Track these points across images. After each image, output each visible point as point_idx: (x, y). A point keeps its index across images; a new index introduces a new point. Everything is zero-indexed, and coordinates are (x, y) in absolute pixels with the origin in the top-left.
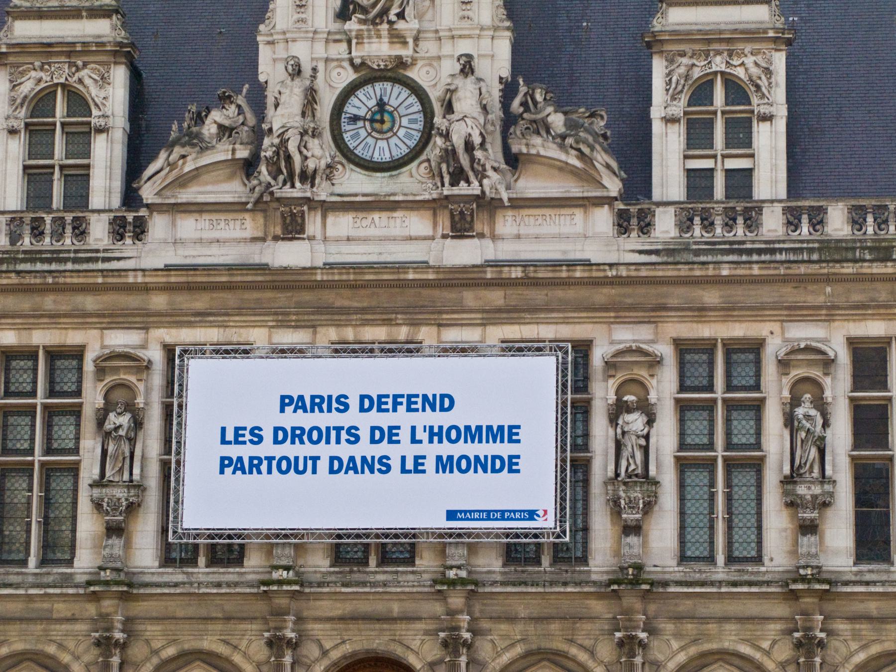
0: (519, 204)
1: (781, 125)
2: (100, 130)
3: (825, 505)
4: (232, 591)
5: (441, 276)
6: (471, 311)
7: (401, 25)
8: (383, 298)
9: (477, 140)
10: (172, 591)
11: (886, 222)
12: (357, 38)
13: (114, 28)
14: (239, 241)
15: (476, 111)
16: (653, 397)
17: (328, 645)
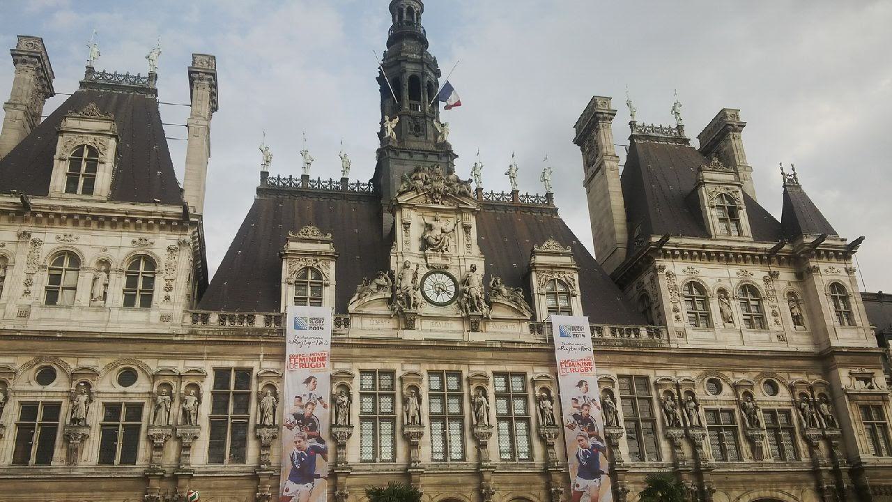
0: (495, 319)
1: (579, 298)
2: (327, 285)
3: (618, 436)
4: (393, 472)
5: (469, 345)
6: (481, 359)
7: (446, 253)
8: (447, 354)
9: (480, 296)
10: (367, 473)
11: (623, 334)
12: (429, 256)
13: (331, 248)
14: (385, 330)
15: (477, 285)
16: (552, 394)
17: (432, 496)
